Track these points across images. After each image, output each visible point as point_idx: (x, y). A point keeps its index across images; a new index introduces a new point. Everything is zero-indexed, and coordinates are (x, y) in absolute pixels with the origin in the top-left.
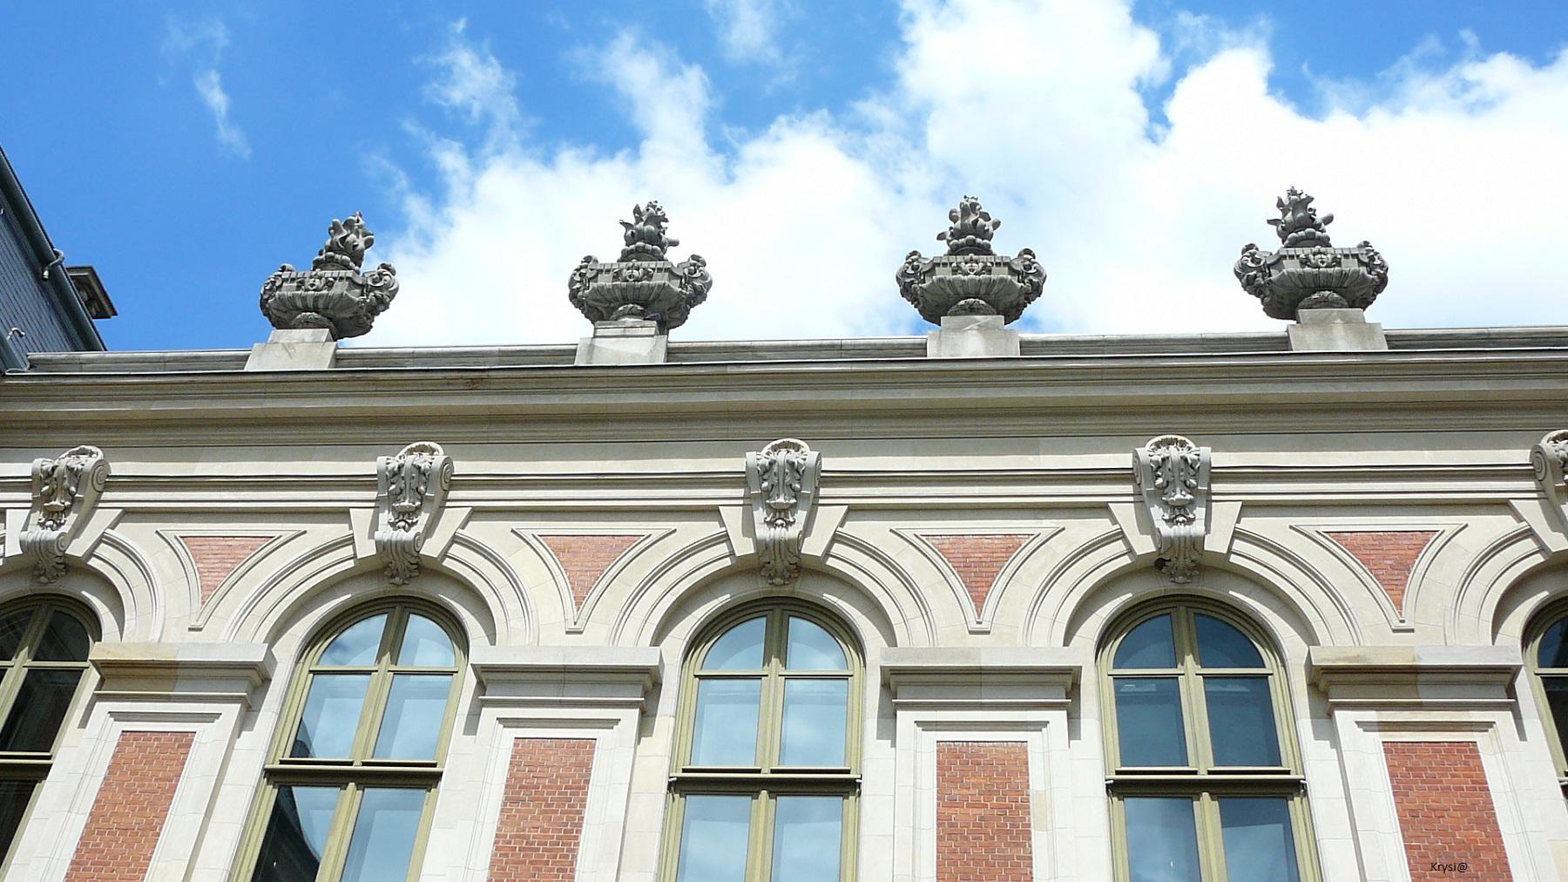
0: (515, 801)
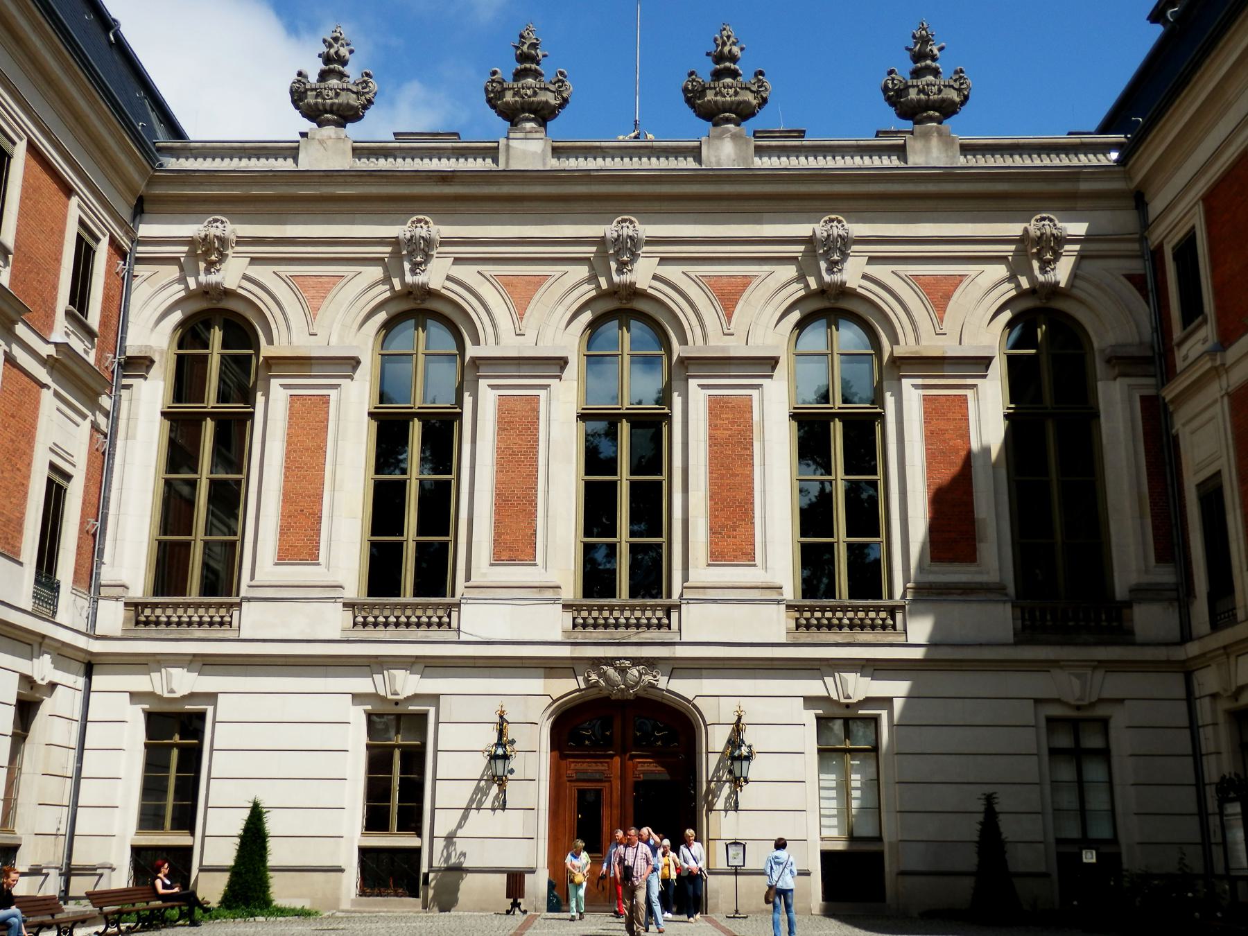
0: (504, 430)
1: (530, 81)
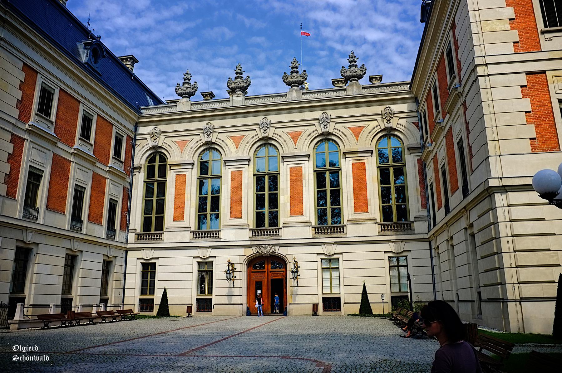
1: (239, 79)
